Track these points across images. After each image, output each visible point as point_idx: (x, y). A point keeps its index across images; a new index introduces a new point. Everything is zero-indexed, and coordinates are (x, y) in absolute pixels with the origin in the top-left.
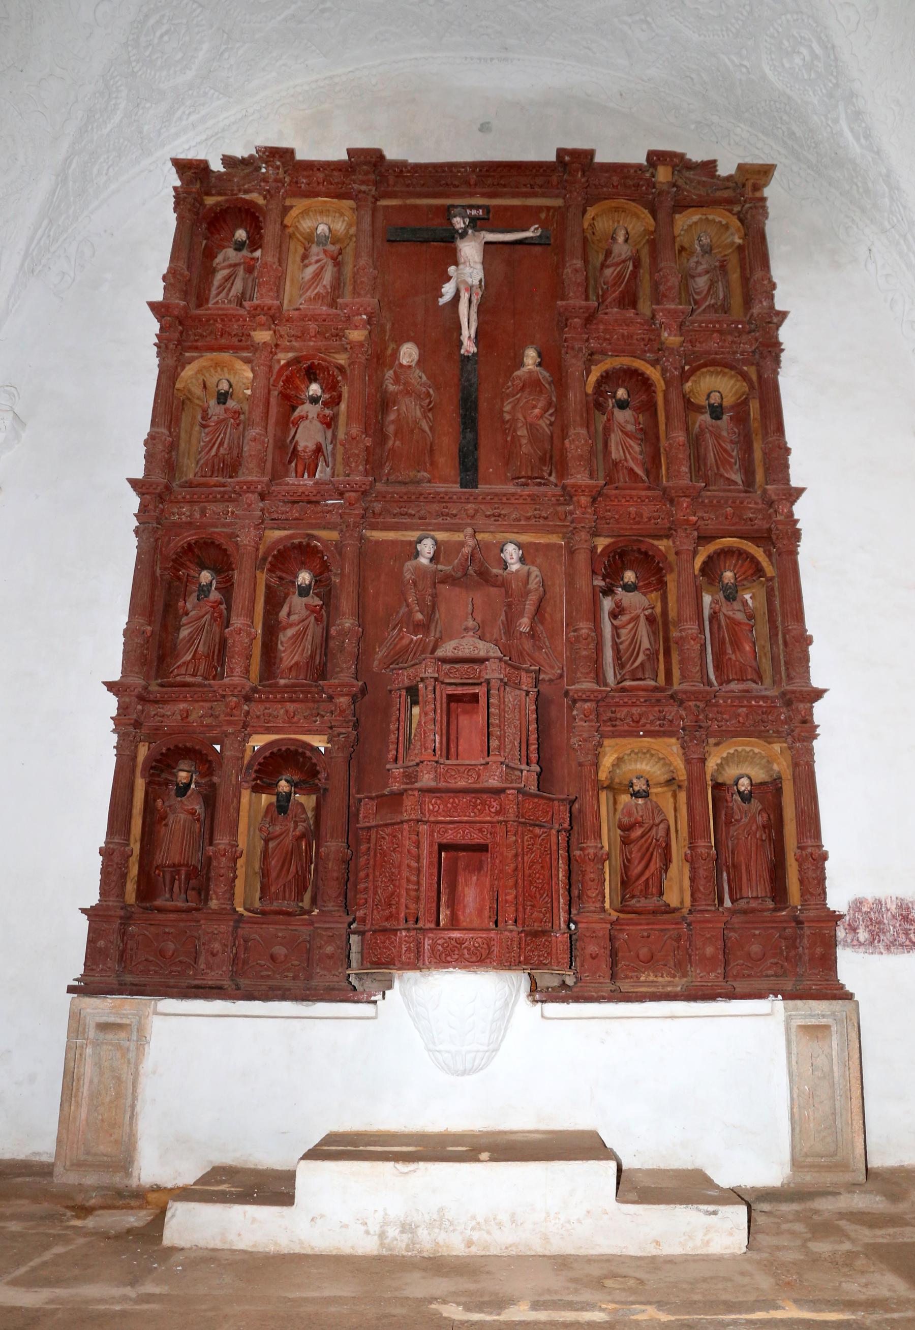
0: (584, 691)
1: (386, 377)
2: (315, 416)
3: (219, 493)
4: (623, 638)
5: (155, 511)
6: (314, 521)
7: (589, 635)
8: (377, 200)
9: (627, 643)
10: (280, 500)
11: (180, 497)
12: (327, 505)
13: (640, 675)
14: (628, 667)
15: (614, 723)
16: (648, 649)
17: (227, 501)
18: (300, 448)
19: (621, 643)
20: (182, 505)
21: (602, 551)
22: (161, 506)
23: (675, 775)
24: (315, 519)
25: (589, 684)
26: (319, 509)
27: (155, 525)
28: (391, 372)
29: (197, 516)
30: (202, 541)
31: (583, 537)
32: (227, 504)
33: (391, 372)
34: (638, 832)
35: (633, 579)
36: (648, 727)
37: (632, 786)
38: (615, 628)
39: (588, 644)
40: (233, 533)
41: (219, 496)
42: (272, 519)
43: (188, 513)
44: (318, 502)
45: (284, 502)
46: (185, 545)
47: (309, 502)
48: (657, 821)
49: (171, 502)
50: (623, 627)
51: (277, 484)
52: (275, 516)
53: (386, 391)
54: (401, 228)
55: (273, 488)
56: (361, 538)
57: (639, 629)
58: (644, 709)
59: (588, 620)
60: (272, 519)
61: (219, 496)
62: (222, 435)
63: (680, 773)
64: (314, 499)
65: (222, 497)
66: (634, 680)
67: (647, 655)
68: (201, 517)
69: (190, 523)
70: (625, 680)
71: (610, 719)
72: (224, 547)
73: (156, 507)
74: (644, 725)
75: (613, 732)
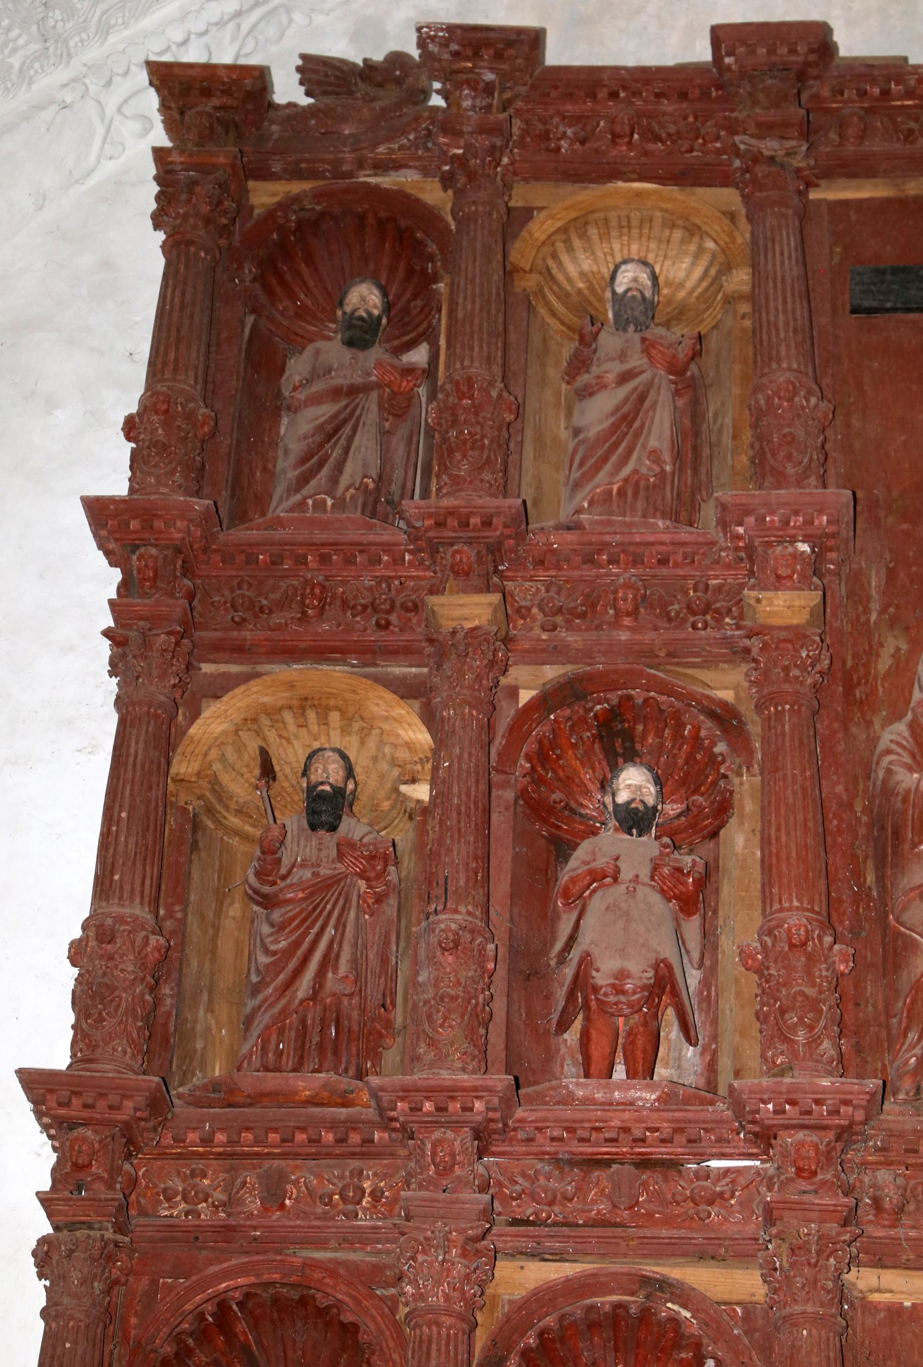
1: (883, 744)
2: (645, 873)
3: (333, 1125)
5: (110, 1186)
6: (664, 1233)
8: (809, 185)
10: (540, 1155)
11: (192, 1136)
12: (707, 1174)
17: (353, 1155)
18: (601, 978)
20: (200, 1165)
22: (127, 1167)
24: (668, 1222)
26: (682, 1187)
27: (109, 1234)
28: (901, 728)
29: (254, 1204)
30: (266, 1295)
32: (356, 1164)
33: (901, 728)
40: (377, 1269)
41: (329, 1137)
42: (515, 1222)
43: (219, 1196)
44: (673, 1165)
45: (555, 1160)
46: (210, 1307)
47: (645, 1163)
49: (161, 1156)
51: (531, 1100)
52: (529, 1211)
53: (887, 791)
54: (895, 271)
55: (520, 1113)
56: (841, 1293)
60: (515, 1222)
61: (329, 1137)
62: (330, 931)
64: (661, 1152)
65: (341, 1141)
68: (265, 1209)
69: (227, 1231)
72: (348, 1318)
73: (115, 1171)
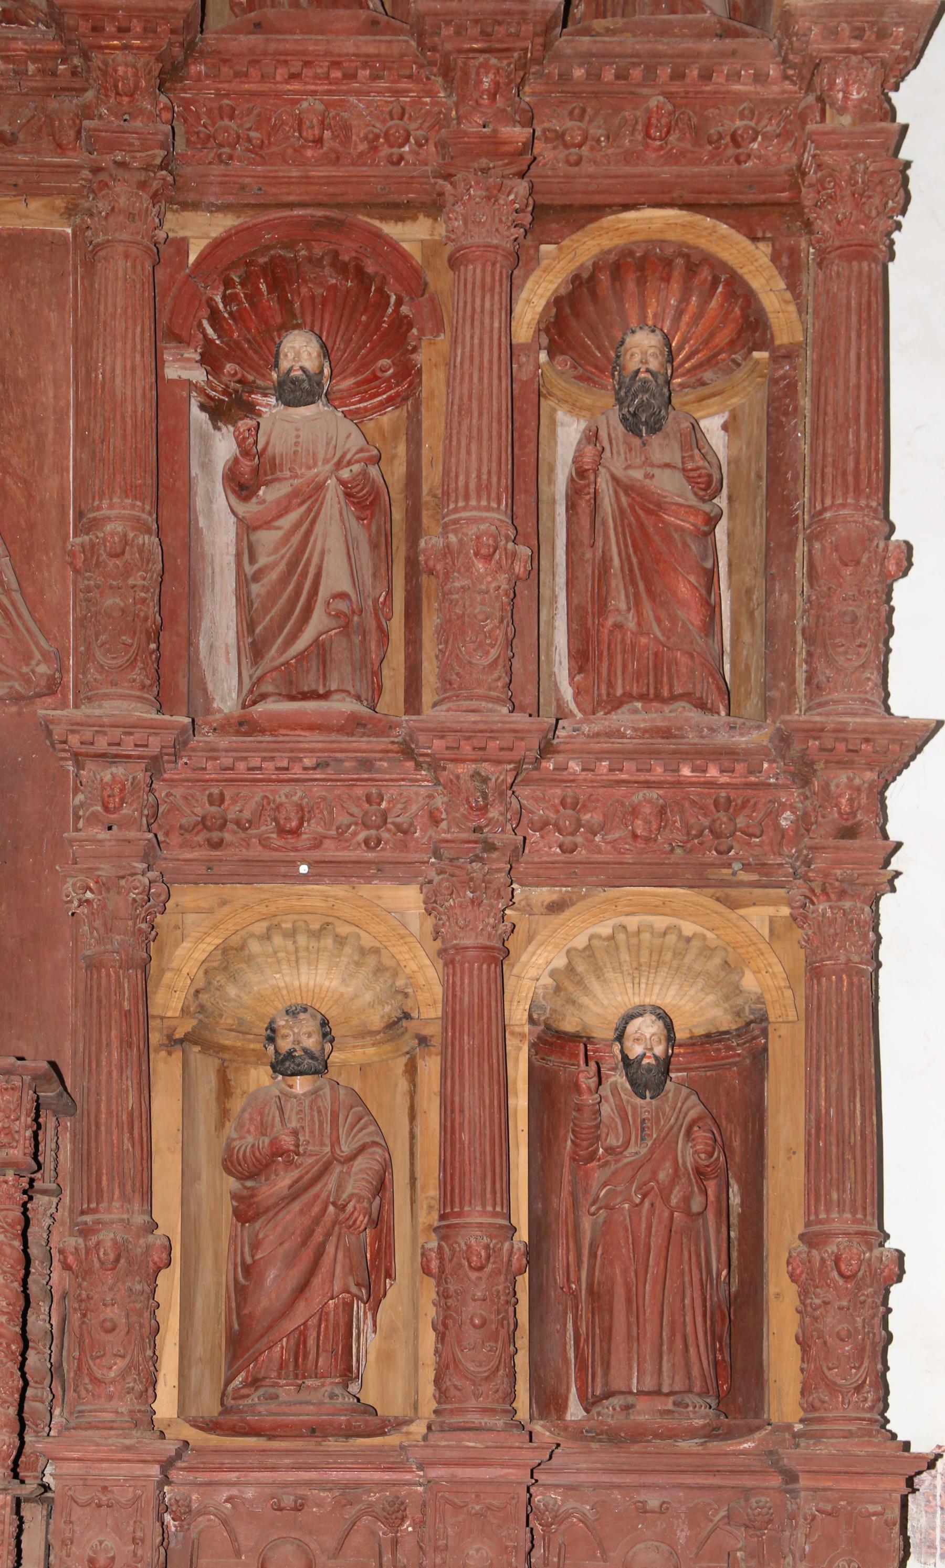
0: (100, 727)
4: (262, 561)
7: (125, 540)
9: (274, 575)
13: (310, 682)
14: (273, 656)
15: (216, 835)
16: (343, 596)
19: (256, 577)
21: (203, 258)
23: (409, 1005)
25: (124, 704)
31: (122, 202)
34: (283, 1181)
35: (311, 365)
36: (330, 851)
37: (271, 1039)
38: (246, 528)
39: (127, 572)
48: (346, 1148)
50: (267, 524)
57: (318, 528)
58: (317, 791)
59: (129, 491)
63: (423, 997)
66: (292, 698)
67: (338, 615)
70: (263, 697)
71: (204, 823)
74: (317, 843)
75: (209, 864)
